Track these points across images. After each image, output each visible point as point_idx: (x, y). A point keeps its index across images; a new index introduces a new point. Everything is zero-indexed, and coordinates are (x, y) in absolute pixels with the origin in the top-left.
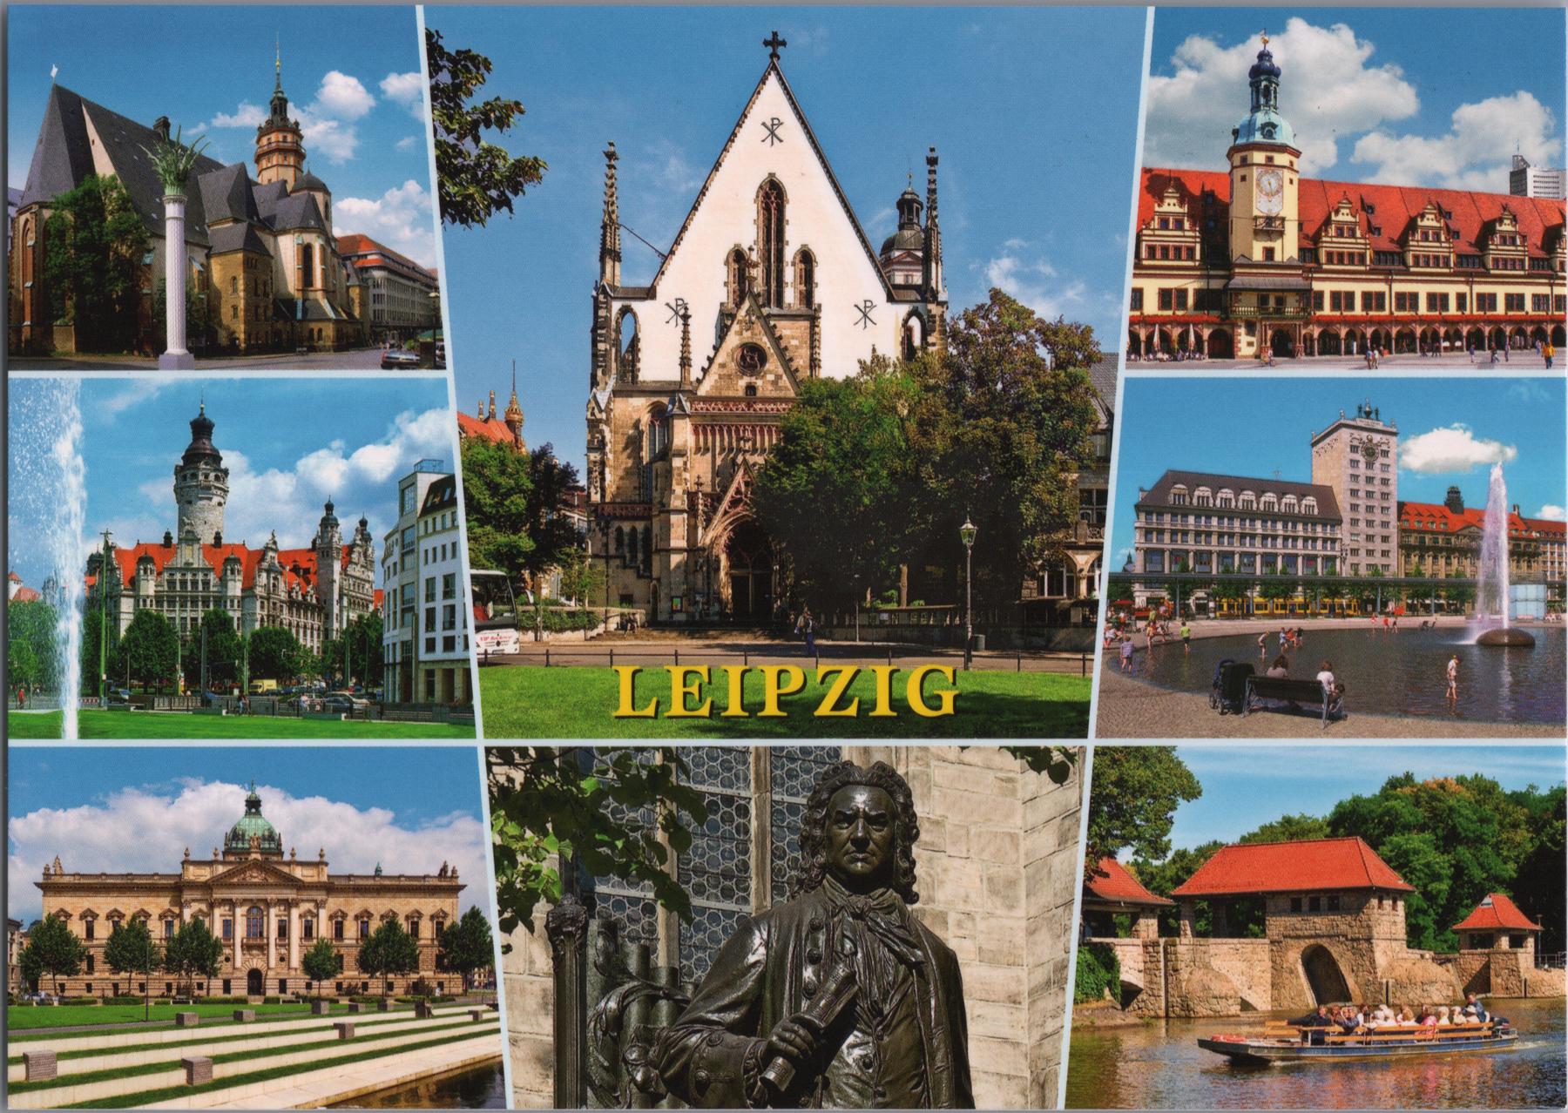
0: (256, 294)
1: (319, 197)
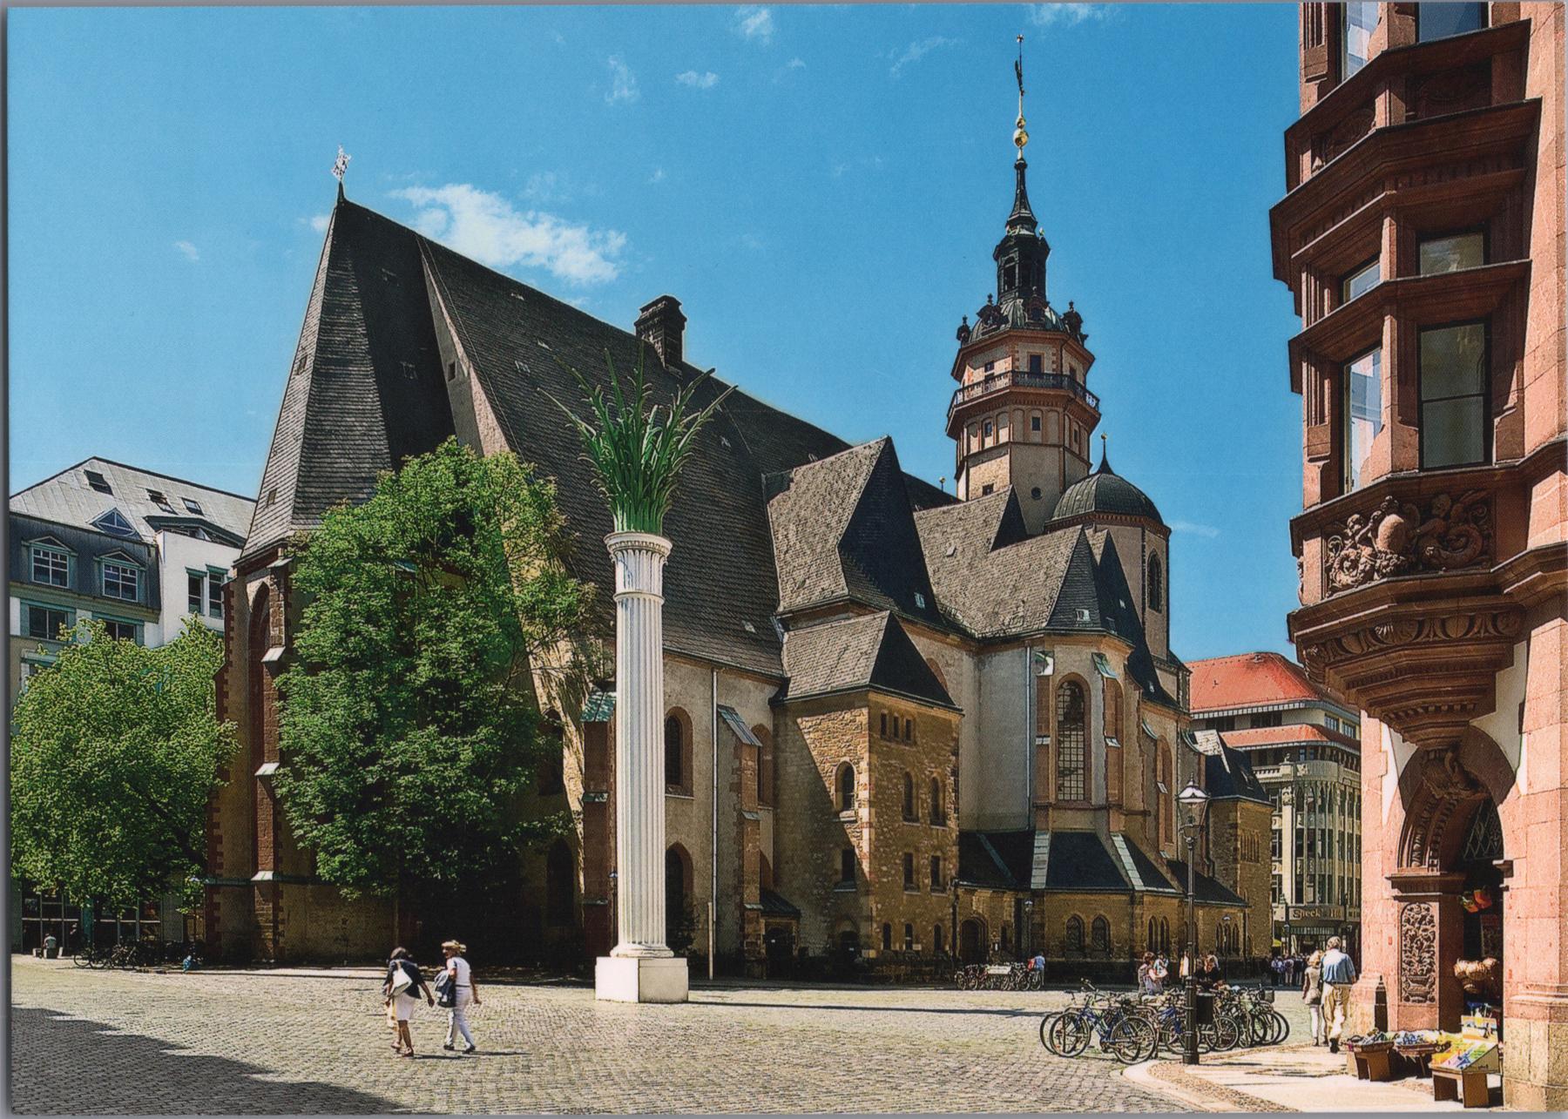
0: (909, 814)
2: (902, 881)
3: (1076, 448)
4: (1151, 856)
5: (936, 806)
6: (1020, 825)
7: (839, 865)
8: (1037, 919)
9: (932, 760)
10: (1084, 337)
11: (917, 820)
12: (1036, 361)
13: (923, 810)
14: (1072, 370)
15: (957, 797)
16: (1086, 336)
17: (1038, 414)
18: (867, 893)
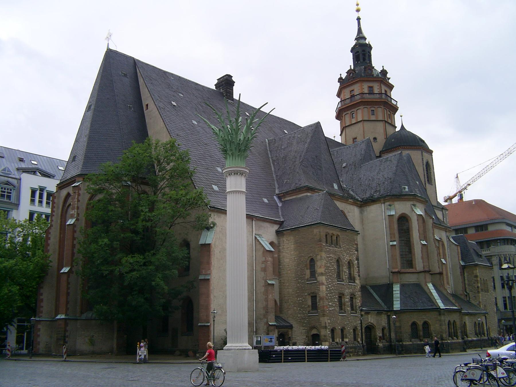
1: (416, 155)
2: (337, 309)
4: (445, 293)
6: (386, 281)
7: (310, 303)
8: (398, 324)
9: (347, 254)
11: (343, 281)
12: (371, 88)
13: (345, 276)
14: (386, 91)
15: (359, 270)
16: (389, 79)
18: (324, 315)
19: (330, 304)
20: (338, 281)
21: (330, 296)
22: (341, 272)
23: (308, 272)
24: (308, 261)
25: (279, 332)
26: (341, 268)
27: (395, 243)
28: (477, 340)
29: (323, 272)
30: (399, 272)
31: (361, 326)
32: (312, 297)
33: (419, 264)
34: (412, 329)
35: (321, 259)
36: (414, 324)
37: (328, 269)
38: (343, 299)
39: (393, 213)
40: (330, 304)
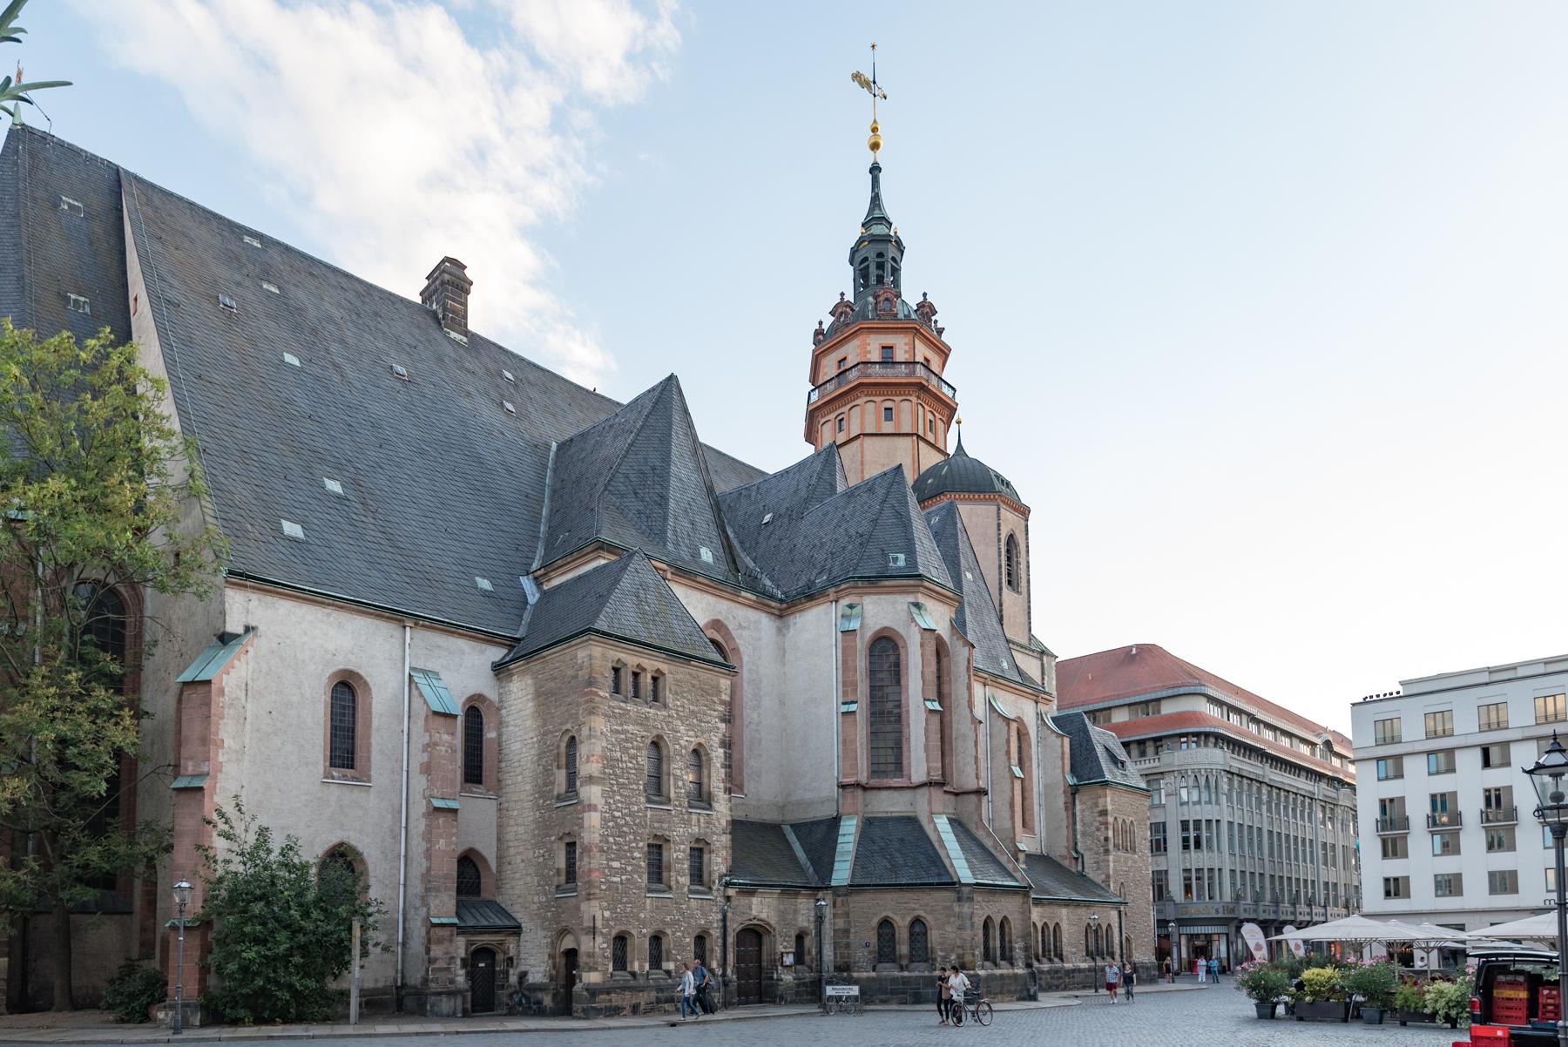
2: (643, 880)
3: (930, 437)
5: (699, 784)
6: (828, 811)
7: (561, 863)
8: (841, 924)
9: (691, 727)
10: (940, 331)
17: (889, 404)
19: (616, 864)
20: (649, 801)
21: (616, 843)
22: (665, 778)
23: (561, 776)
24: (563, 745)
25: (469, 944)
26: (665, 767)
27: (853, 707)
28: (1089, 970)
29: (596, 774)
30: (865, 788)
31: (725, 927)
32: (568, 844)
33: (919, 765)
34: (880, 935)
35: (590, 737)
36: (886, 923)
37: (613, 767)
38: (665, 854)
39: (855, 624)
40: (616, 864)
